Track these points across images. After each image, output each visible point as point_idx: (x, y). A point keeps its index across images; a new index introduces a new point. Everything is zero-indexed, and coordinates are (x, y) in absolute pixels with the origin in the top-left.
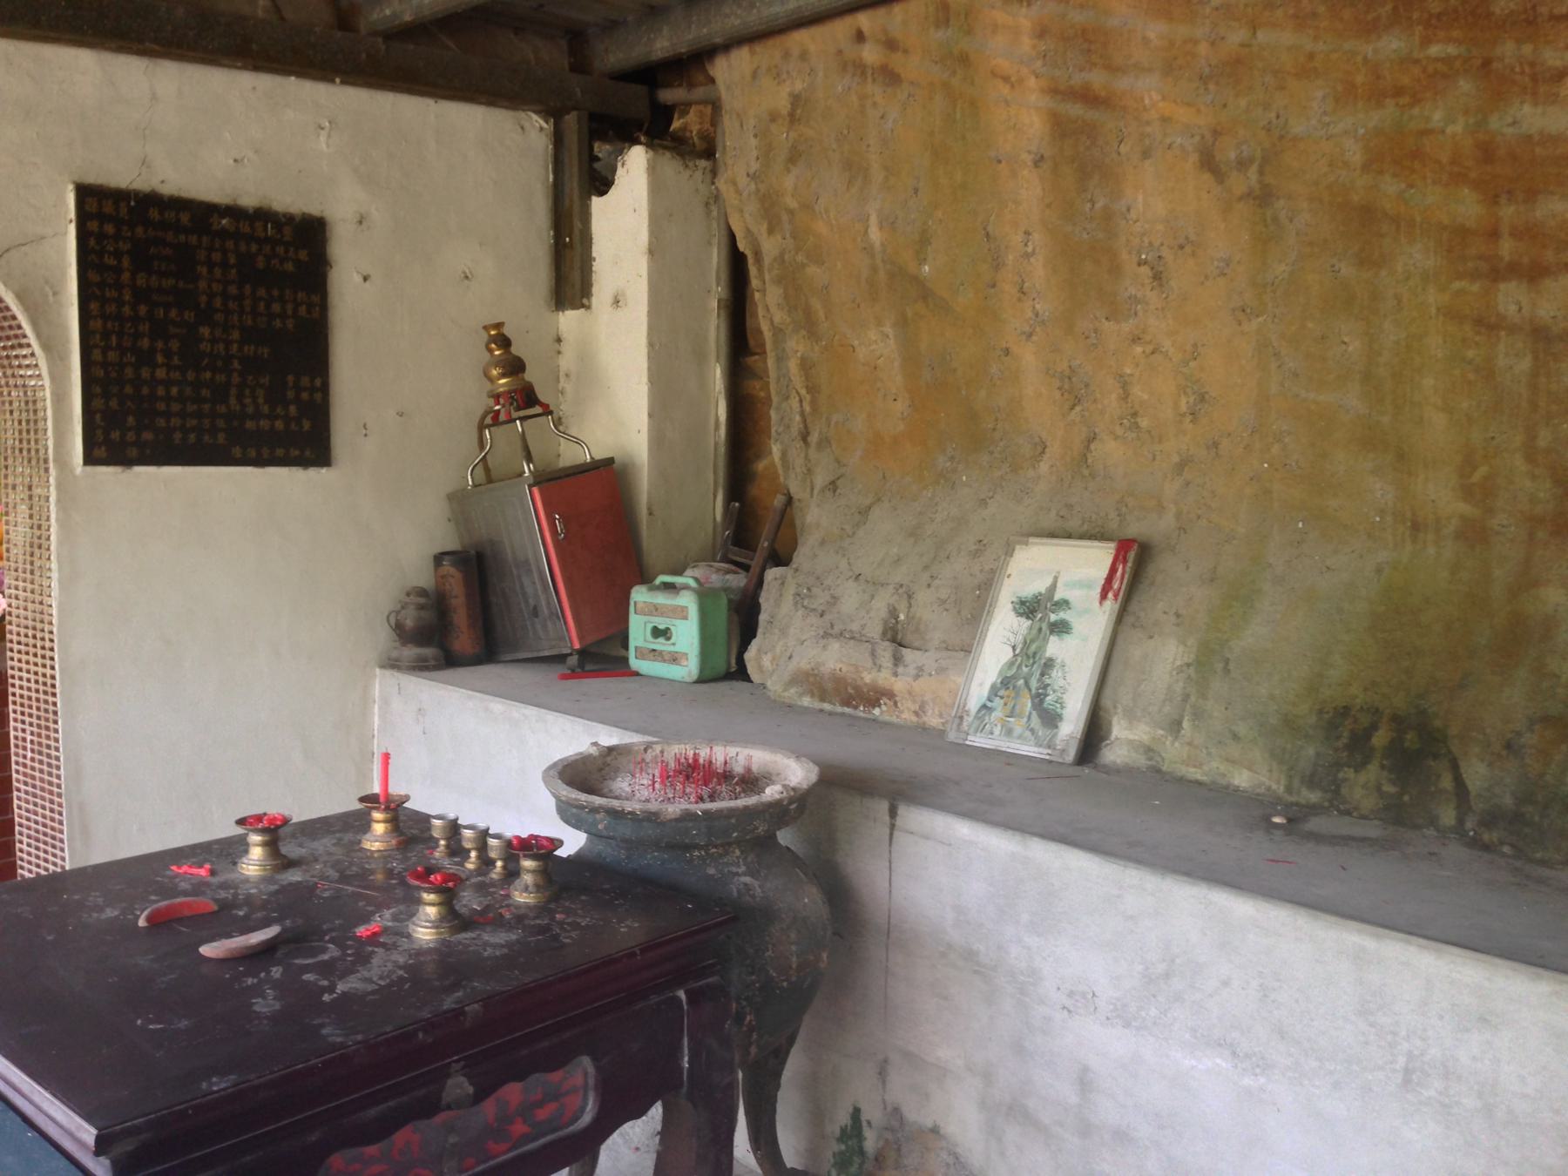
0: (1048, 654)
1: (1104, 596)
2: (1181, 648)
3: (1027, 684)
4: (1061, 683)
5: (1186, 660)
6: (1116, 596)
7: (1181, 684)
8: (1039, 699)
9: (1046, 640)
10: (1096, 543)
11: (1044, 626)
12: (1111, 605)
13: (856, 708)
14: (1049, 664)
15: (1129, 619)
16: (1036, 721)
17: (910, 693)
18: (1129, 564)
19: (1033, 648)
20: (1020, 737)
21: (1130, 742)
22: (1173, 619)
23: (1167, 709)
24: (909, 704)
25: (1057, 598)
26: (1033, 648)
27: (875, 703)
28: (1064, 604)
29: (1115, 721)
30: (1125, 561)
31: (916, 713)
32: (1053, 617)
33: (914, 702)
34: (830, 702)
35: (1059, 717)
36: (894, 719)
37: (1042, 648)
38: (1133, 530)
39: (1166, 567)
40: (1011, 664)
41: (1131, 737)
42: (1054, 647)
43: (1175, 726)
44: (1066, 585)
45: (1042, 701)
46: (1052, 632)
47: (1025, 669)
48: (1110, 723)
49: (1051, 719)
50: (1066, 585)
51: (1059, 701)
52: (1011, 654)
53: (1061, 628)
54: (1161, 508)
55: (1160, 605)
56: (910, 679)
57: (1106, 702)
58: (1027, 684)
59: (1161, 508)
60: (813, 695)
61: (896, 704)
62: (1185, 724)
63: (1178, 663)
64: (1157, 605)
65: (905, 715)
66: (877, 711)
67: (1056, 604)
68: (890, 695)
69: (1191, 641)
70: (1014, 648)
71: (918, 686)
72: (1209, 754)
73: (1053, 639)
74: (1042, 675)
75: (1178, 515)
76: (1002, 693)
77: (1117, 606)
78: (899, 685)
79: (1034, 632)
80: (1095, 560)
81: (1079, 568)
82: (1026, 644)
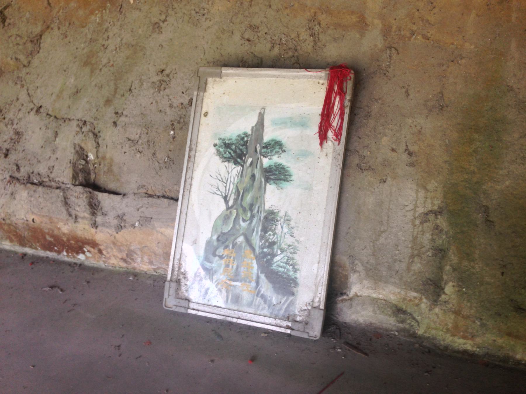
0: (267, 207)
1: (323, 137)
2: (422, 193)
3: (248, 241)
4: (289, 240)
5: (429, 207)
6: (338, 135)
7: (428, 236)
8: (265, 261)
9: (262, 190)
10: (303, 73)
11: (258, 173)
12: (333, 147)
13: (59, 252)
14: (271, 218)
15: (355, 160)
16: (266, 287)
17: (114, 243)
18: (348, 97)
19: (248, 198)
20: (250, 304)
21: (374, 301)
22: (405, 157)
23: (417, 266)
24: (115, 252)
25: (267, 138)
26: (248, 198)
27: (79, 250)
28: (276, 146)
29: (353, 278)
30: (342, 93)
31: (125, 260)
32: (266, 162)
33: (120, 251)
34: (31, 247)
35: (295, 282)
36: (101, 264)
37: (259, 198)
38: (333, 52)
39: (384, 92)
40: (225, 218)
41: (375, 295)
42: (273, 197)
43: (433, 288)
44: (275, 123)
45: (269, 262)
46: (267, 180)
47: (244, 225)
48: (347, 277)
49: (285, 284)
50: (275, 123)
51: (291, 262)
52: (223, 207)
53: (277, 175)
54: (362, 25)
55: (385, 141)
56: (112, 231)
57: (343, 259)
58: (248, 241)
59: (362, 25)
60: (11, 241)
61: (100, 252)
62: (449, 289)
63: (420, 210)
64: (383, 144)
65: (113, 261)
66: (81, 257)
67: (267, 146)
68: (94, 244)
69: (432, 185)
70: (226, 199)
71: (123, 236)
72: (483, 325)
73: (271, 188)
74: (265, 230)
75: (386, 32)
76: (221, 251)
77: (341, 148)
78: (101, 236)
79: (247, 179)
80: (300, 95)
81: (289, 103)
82: (240, 195)
